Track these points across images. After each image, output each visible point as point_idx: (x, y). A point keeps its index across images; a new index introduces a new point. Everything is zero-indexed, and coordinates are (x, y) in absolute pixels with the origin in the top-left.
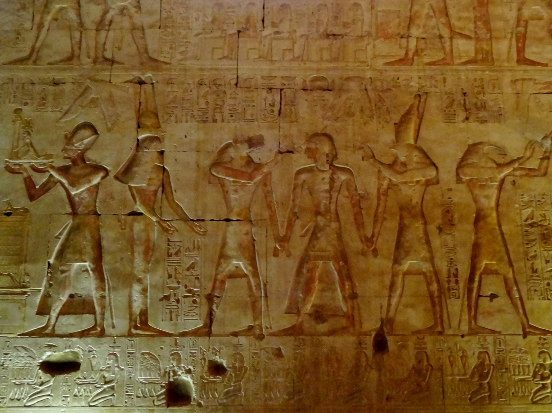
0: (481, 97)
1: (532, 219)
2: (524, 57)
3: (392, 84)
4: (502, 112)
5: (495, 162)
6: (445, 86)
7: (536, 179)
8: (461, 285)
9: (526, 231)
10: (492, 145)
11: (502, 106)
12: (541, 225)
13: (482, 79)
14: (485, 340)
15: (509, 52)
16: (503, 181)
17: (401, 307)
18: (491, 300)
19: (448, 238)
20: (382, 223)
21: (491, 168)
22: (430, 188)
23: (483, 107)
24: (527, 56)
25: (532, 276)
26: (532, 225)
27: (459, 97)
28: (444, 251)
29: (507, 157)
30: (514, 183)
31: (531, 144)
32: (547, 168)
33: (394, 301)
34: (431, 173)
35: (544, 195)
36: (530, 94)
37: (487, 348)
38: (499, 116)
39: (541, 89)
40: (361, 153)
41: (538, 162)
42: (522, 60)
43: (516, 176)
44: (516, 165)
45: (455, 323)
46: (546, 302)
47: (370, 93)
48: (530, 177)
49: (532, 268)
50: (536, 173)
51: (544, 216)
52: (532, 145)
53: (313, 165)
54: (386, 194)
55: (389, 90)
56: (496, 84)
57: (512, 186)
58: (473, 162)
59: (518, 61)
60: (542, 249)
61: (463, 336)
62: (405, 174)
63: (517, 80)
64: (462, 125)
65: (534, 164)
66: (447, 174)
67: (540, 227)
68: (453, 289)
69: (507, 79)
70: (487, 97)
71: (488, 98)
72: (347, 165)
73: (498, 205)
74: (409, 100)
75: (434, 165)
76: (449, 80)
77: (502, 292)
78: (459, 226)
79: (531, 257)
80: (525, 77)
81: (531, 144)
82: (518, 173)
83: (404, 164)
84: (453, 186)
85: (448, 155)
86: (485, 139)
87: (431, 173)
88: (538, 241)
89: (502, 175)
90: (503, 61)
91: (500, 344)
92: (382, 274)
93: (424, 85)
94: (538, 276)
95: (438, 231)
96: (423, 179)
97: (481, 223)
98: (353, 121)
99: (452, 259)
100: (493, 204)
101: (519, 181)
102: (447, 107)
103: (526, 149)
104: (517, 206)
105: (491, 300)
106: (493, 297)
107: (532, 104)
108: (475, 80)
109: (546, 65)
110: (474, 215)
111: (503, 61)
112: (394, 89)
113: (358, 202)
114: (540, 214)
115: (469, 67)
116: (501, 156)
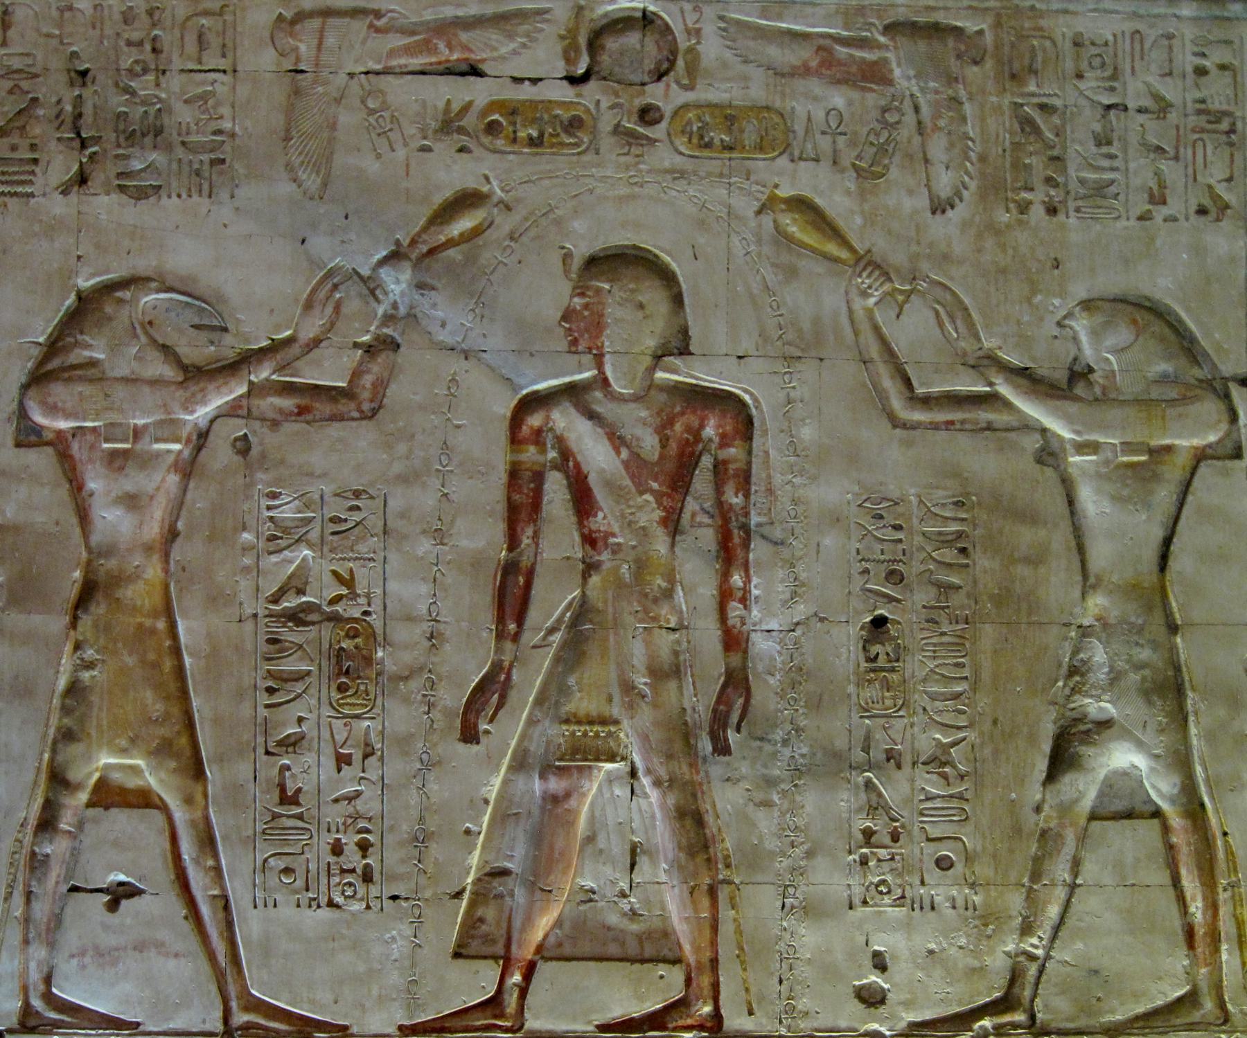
1: (301, 592)
16: (203, 436)
29: (228, 339)
38: (211, 169)
44: (264, 373)
57: (238, 459)
86: (142, 264)
89: (202, 413)
103: (309, 306)
104: (247, 536)
107: (347, 118)
116: (204, 336)
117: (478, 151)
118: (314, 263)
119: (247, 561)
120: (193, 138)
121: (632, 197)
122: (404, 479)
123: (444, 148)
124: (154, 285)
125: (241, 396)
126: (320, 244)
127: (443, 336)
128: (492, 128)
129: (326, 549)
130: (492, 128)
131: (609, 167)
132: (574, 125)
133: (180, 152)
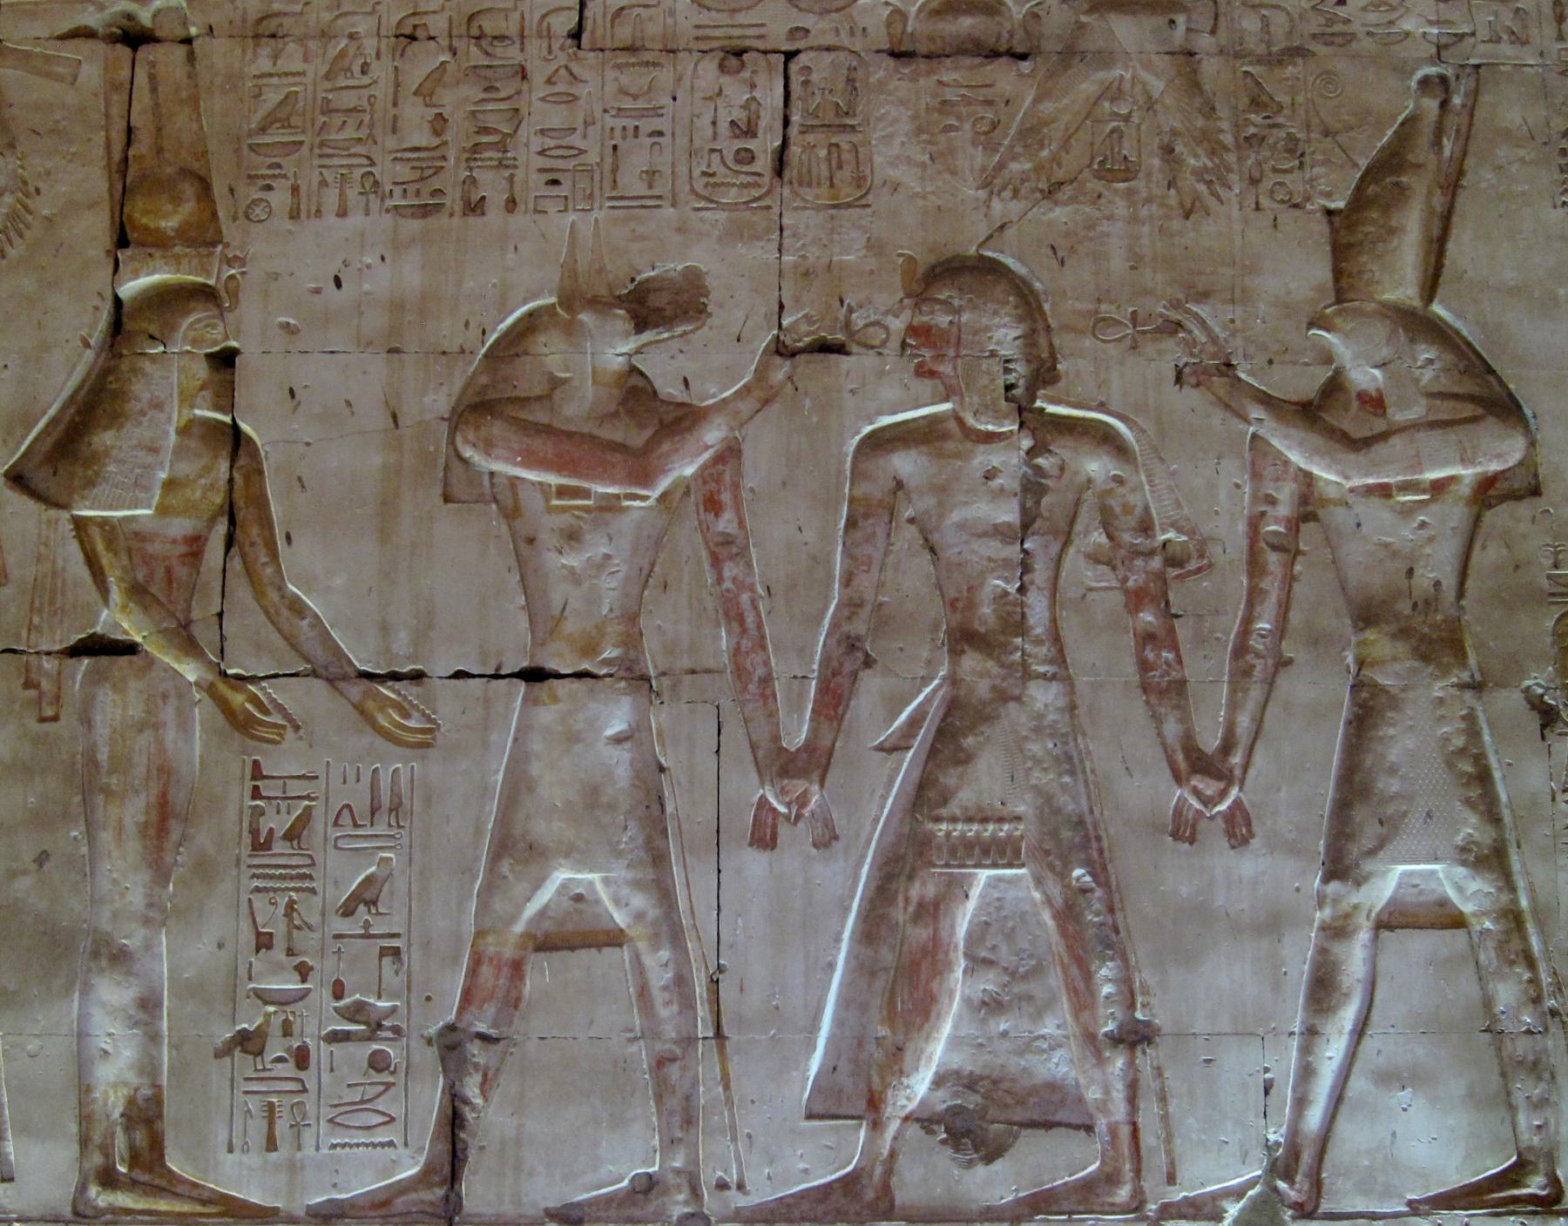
17: (1359, 1084)
20: (1271, 684)
22: (1499, 517)
34: (1501, 452)
40: (1172, 353)
47: (1210, 67)
62: (1380, 450)
72: (1102, 407)
74: (1400, 100)
83: (1374, 403)
87: (1501, 452)
93: (1466, 29)
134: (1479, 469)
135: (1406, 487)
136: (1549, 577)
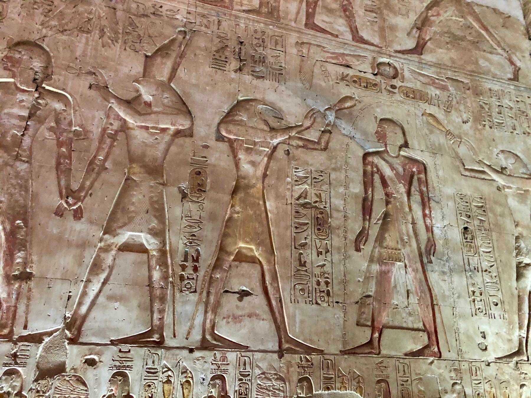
0: (260, 50)
1: (305, 198)
2: (314, 23)
3: (152, 10)
4: (283, 72)
5: (266, 123)
6: (218, 29)
7: (315, 153)
8: (201, 273)
9: (297, 212)
10: (266, 105)
11: (283, 65)
12: (316, 207)
13: (263, 33)
14: (224, 358)
15: (298, 13)
16: (275, 148)
17: (101, 299)
18: (240, 299)
19: (193, 207)
20: (98, 174)
21: (263, 130)
22: (180, 140)
23: (262, 61)
24: (316, 22)
25: (299, 270)
26: (304, 205)
27: (233, 44)
28: (185, 223)
29: (283, 122)
30: (288, 153)
31: (311, 114)
32: (328, 143)
33: (94, 288)
34: (183, 124)
35: (322, 172)
36: (317, 60)
37: (225, 371)
38: (279, 75)
39: (328, 57)
40: (91, 79)
41: (318, 134)
42: (310, 24)
43: (293, 146)
44: (293, 133)
45: (182, 330)
46: (315, 306)
47: (119, 14)
48: (307, 149)
49: (300, 260)
50: (316, 146)
51: (319, 196)
52: (314, 113)
53: (12, 80)
54: (113, 137)
55: (147, 16)
56: (279, 42)
57: (285, 156)
58: (241, 120)
59: (306, 25)
60: (314, 237)
61: (191, 351)
62: (148, 117)
63: (303, 43)
64: (233, 75)
65: (313, 135)
66: (204, 130)
67: (314, 209)
68: (188, 278)
69: (293, 38)
70: (268, 53)
71: (269, 53)
72: (63, 90)
73: (265, 176)
74: (170, 33)
75: (190, 113)
76: (224, 24)
77: (255, 286)
78: (211, 194)
79: (300, 245)
80: (313, 42)
81: (311, 114)
82: (294, 143)
83: (149, 105)
84: (212, 143)
85: (209, 105)
86: (259, 96)
87: (183, 124)
88: (310, 225)
89: (275, 142)
90: (291, 20)
91: (245, 364)
92: (83, 245)
93: (193, 21)
94: (306, 271)
95: (181, 196)
96: (173, 128)
97: (241, 195)
98: (87, 39)
99: (194, 235)
100: (260, 172)
101: (293, 151)
102: (217, 51)
103: (306, 117)
104: (289, 179)
105: (240, 299)
106: (243, 294)
107: (317, 70)
108: (256, 31)
109: (337, 36)
110: (234, 183)
111: (291, 20)
112: (152, 16)
113: (69, 142)
114: (315, 194)
115: (251, 16)
116: (277, 120)
117: (351, 86)
118: (308, 106)
119: (289, 187)
120: (274, 66)
121: (391, 105)
122: (334, 169)
123: (342, 84)
124: (262, 103)
125: (287, 139)
126: (310, 102)
127: (344, 132)
128: (355, 82)
129: (313, 186)
130: (355, 82)
131: (384, 97)
132: (375, 85)
133: (270, 69)
134: (176, 127)
135: (153, 128)
136: (191, 159)
